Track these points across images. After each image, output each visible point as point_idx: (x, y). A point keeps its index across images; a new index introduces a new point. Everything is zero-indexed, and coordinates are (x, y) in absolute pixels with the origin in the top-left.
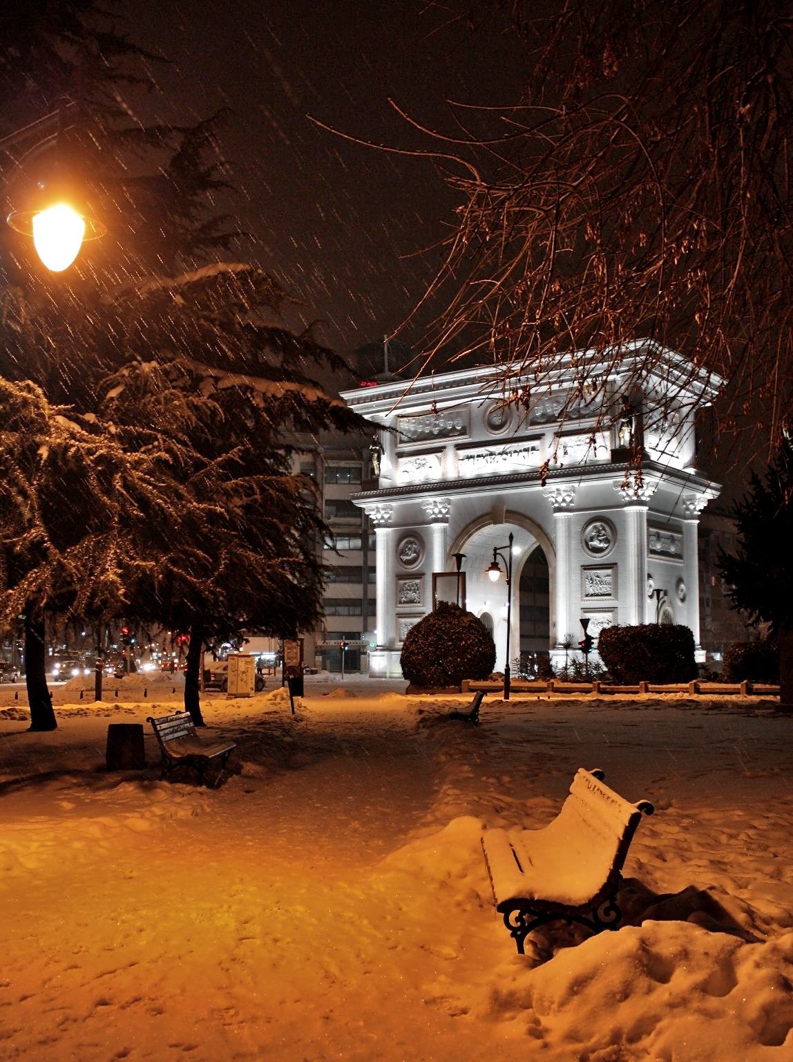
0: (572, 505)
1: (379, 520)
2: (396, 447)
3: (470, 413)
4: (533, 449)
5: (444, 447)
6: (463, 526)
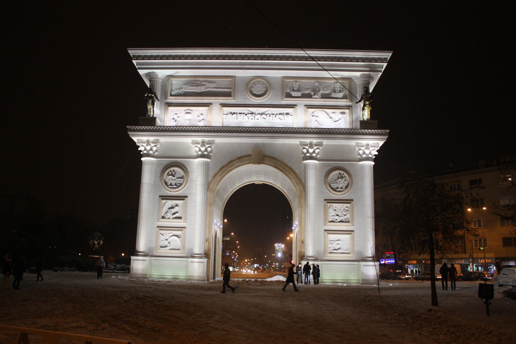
0: (319, 156)
1: (148, 151)
2: (166, 98)
3: (235, 83)
4: (287, 114)
5: (211, 104)
6: (224, 164)
